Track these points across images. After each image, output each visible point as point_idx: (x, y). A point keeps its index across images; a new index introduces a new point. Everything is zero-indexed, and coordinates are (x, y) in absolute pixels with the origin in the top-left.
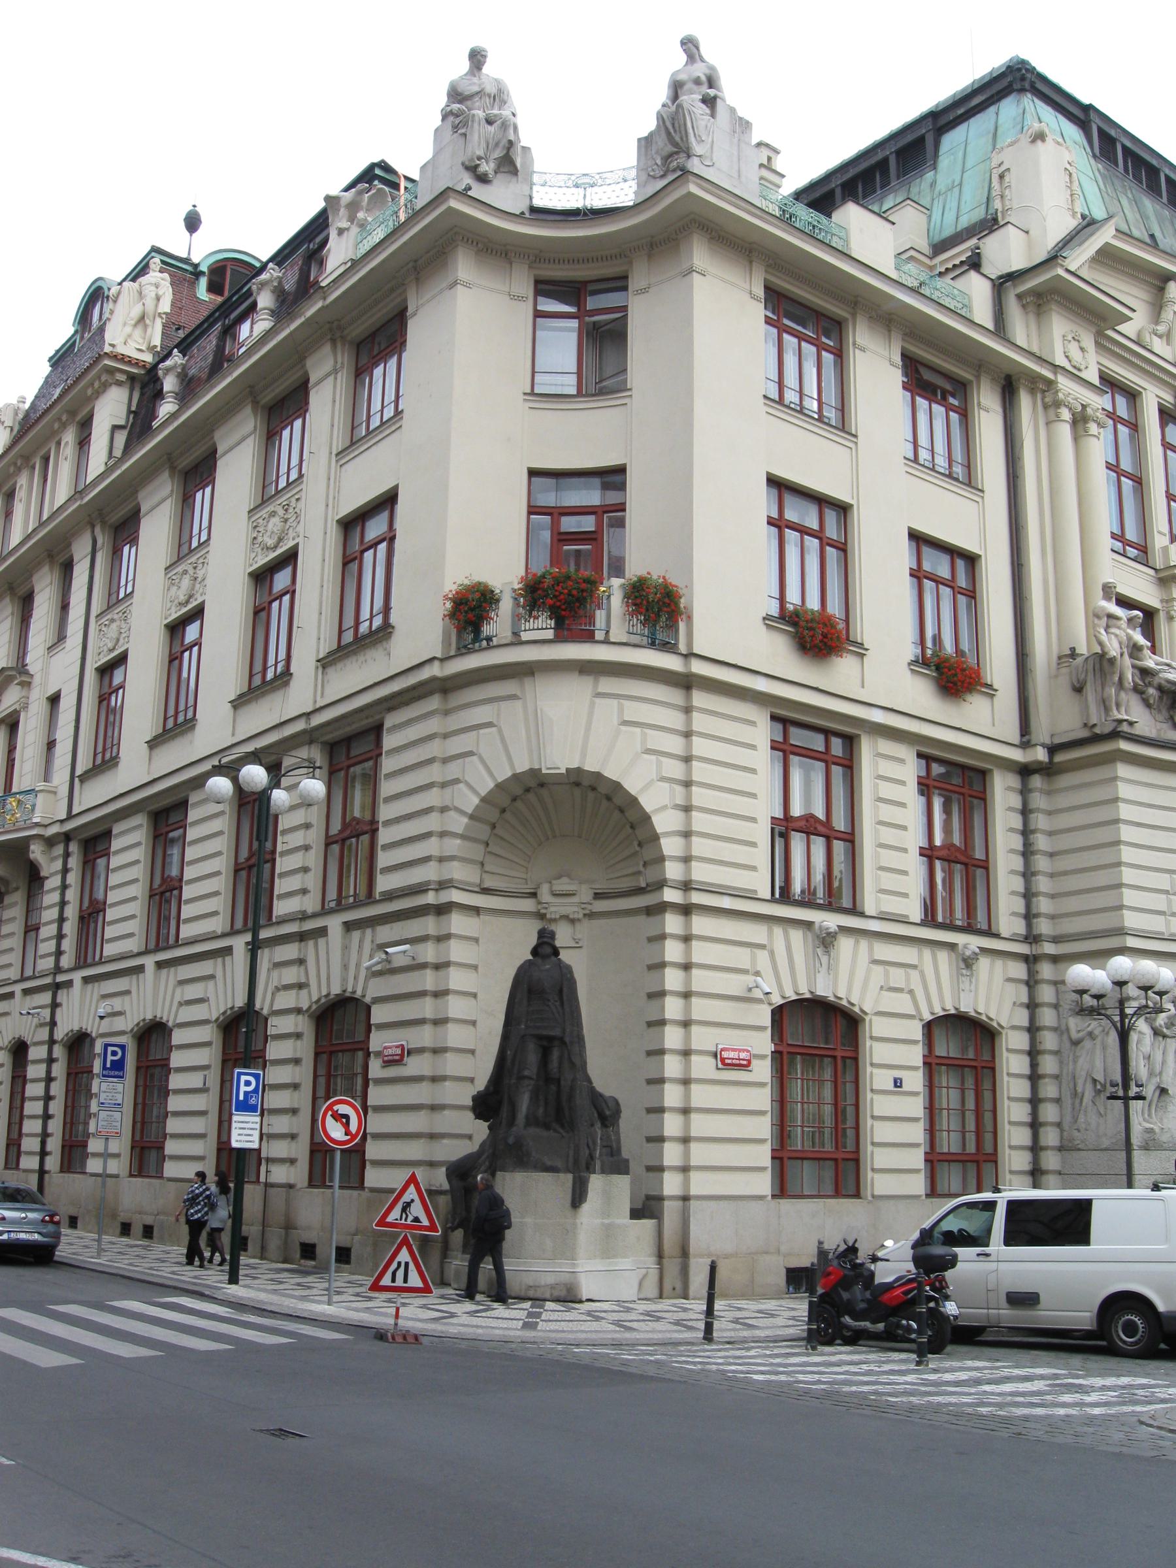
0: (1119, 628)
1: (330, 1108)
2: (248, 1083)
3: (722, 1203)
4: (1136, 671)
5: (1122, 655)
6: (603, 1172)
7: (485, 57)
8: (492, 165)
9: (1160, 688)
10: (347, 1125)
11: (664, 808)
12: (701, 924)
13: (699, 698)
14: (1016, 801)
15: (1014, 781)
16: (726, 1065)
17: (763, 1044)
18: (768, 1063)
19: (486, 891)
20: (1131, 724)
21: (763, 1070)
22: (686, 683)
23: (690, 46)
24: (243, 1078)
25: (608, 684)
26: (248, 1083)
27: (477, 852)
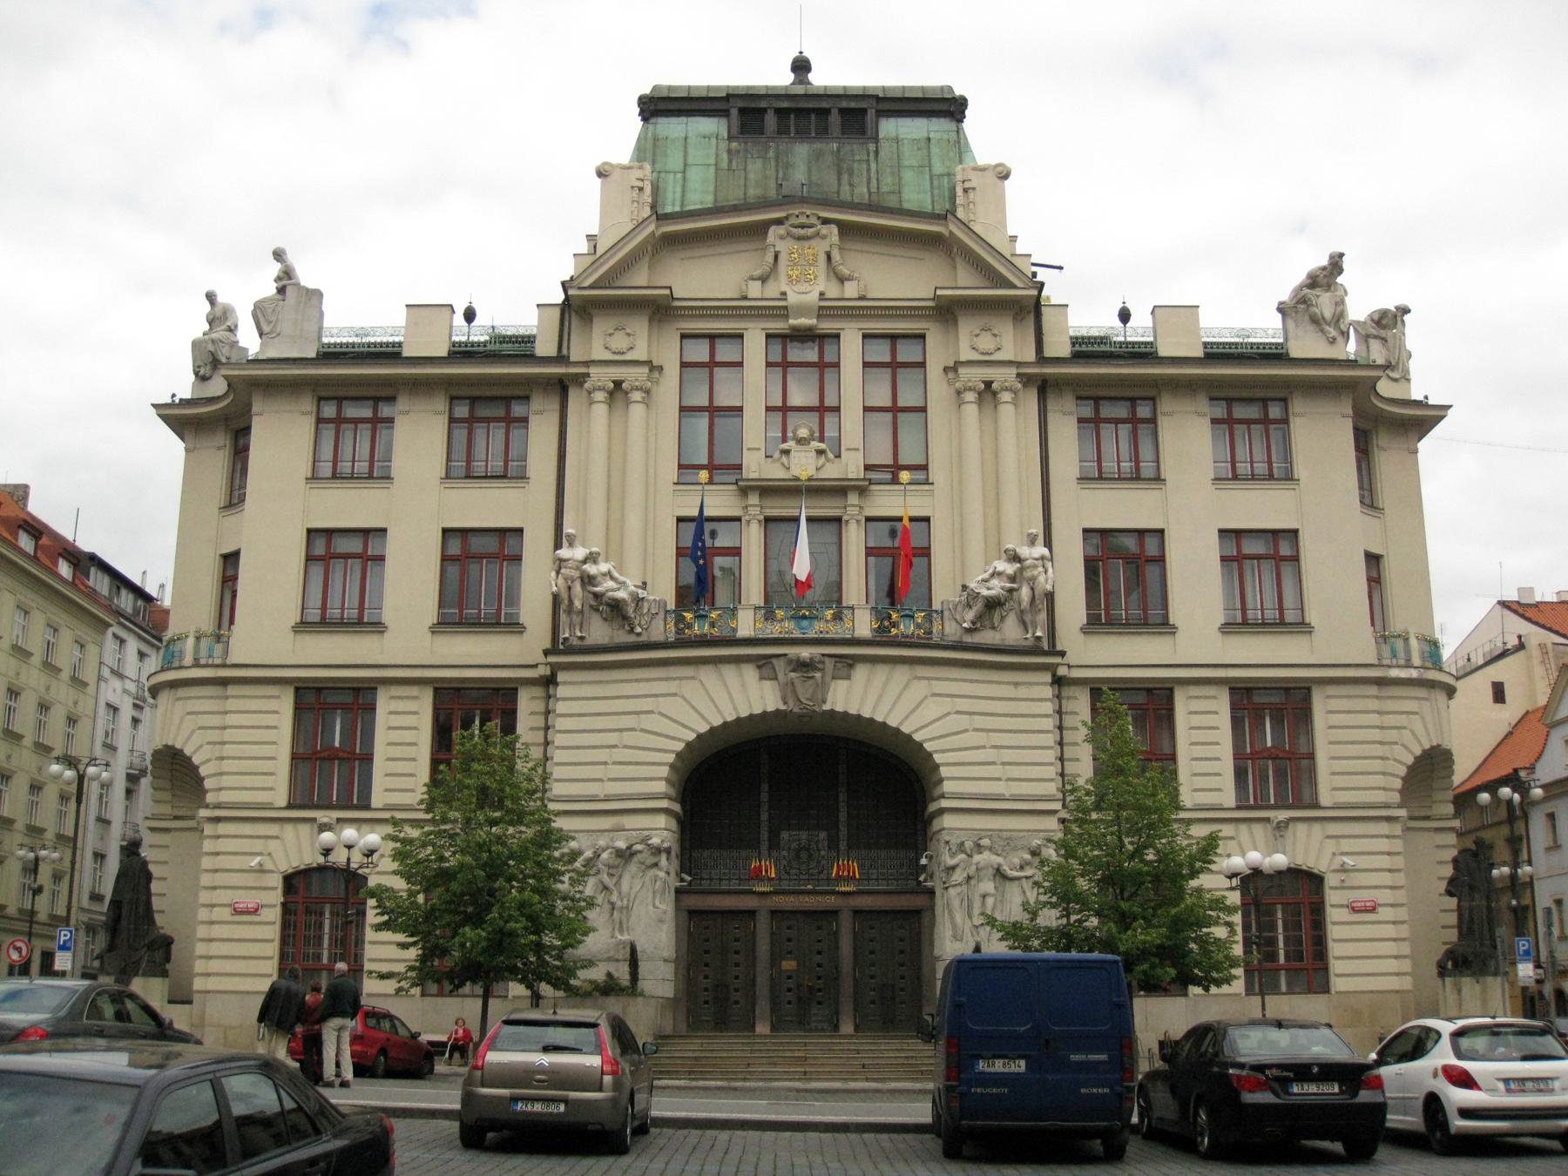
0: (566, 567)
1: (12, 943)
2: (65, 935)
3: (233, 997)
4: (591, 596)
5: (569, 588)
6: (144, 975)
7: (215, 296)
8: (208, 367)
9: (608, 605)
10: (20, 952)
11: (209, 760)
12: (223, 828)
13: (232, 690)
14: (539, 706)
15: (539, 691)
16: (237, 912)
17: (277, 897)
18: (278, 910)
19: (177, 818)
20: (582, 638)
21: (274, 914)
22: (224, 682)
23: (278, 255)
24: (63, 933)
25: (183, 692)
26: (65, 935)
27: (167, 796)
